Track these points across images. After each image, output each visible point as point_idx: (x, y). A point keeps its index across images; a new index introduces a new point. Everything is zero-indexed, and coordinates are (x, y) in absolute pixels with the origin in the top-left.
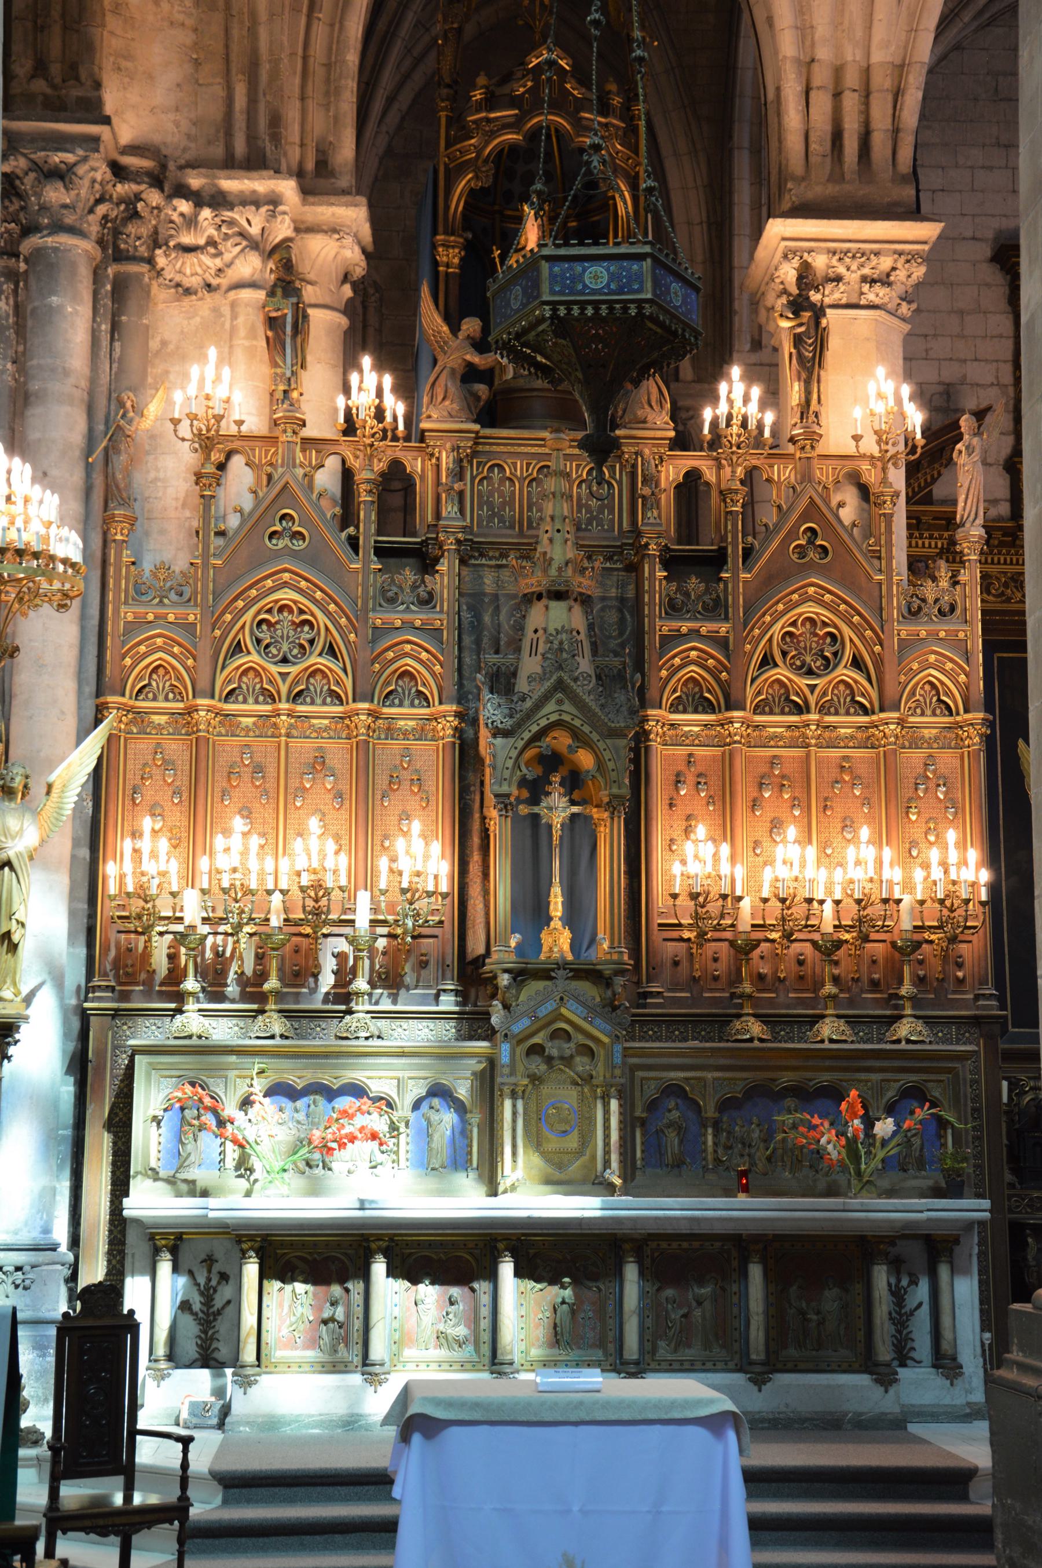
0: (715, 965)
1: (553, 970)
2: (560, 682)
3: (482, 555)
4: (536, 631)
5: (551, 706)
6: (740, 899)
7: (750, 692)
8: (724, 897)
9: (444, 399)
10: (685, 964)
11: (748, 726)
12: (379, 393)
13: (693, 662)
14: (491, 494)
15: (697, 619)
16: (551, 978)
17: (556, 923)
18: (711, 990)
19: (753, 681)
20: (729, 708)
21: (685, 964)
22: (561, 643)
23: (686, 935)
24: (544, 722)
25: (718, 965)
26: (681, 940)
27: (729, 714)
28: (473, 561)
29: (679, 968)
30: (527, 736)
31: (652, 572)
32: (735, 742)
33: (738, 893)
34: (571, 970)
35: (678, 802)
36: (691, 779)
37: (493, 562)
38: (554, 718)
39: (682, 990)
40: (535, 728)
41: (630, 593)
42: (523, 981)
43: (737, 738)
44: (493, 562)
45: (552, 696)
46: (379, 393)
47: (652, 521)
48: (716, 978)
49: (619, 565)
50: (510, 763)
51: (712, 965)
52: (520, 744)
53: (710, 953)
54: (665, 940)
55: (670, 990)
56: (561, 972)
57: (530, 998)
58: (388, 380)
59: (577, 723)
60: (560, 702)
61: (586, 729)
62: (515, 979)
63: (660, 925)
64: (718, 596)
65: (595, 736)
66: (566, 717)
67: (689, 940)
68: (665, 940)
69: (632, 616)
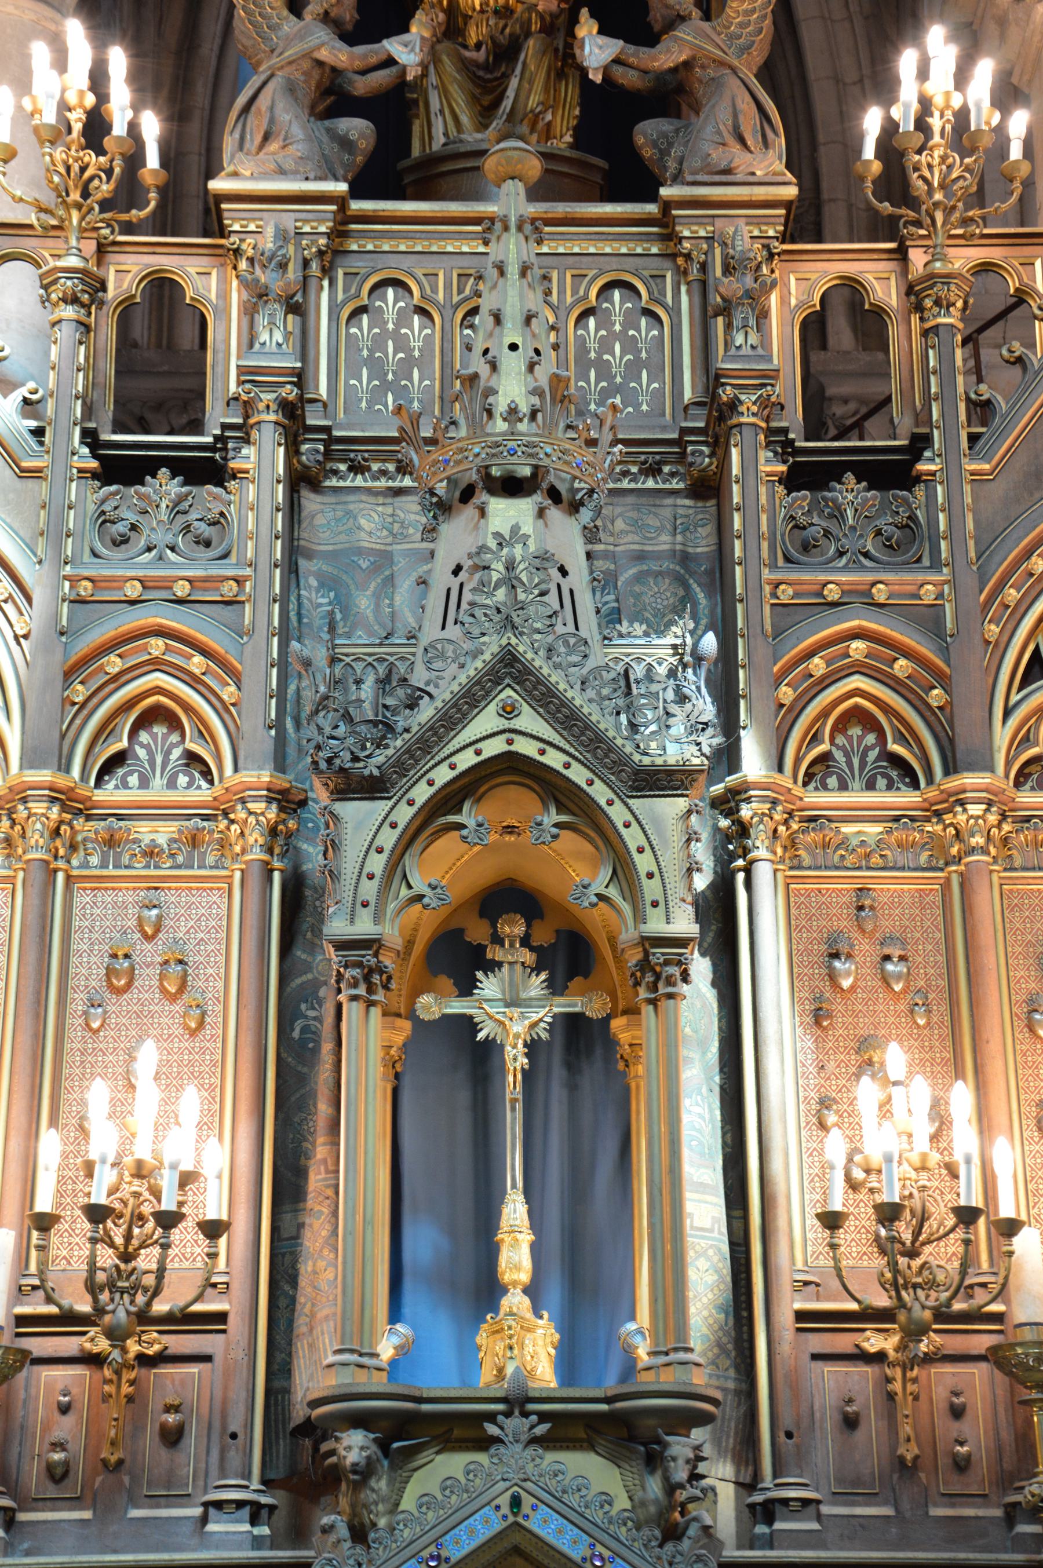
0: (955, 1428)
1: (491, 1417)
2: (509, 659)
3: (356, 469)
4: (457, 571)
5: (487, 720)
6: (1010, 1228)
7: (1002, 736)
8: (967, 1216)
9: (266, 137)
10: (873, 1424)
11: (1004, 817)
12: (98, 80)
13: (858, 669)
14: (379, 343)
15: (863, 568)
16: (485, 1443)
17: (515, 1301)
18: (952, 1498)
19: (1007, 713)
20: (951, 768)
21: (873, 1424)
22: (510, 566)
23: (874, 1342)
24: (467, 760)
25: (964, 1427)
26: (863, 1357)
27: (954, 783)
28: (334, 482)
29: (860, 1434)
30: (422, 793)
31: (749, 464)
32: (972, 851)
33: (1006, 1210)
34: (543, 1417)
35: (838, 1007)
36: (866, 949)
37: (383, 483)
38: (493, 748)
39: (870, 1498)
40: (443, 775)
41: (703, 544)
42: (410, 1453)
43: (978, 840)
44: (383, 483)
45: (487, 696)
46: (98, 80)
47: (746, 351)
48: (962, 1465)
49: (676, 484)
50: (377, 864)
51: (947, 1428)
52: (404, 814)
53: (940, 1394)
54: (815, 1357)
55: (837, 1497)
56: (515, 1424)
57: (426, 1502)
58: (118, 60)
59: (554, 760)
60: (508, 711)
61: (578, 775)
62: (384, 1446)
63: (801, 1316)
64: (913, 518)
65: (600, 793)
66: (526, 748)
67: (880, 1357)
68: (815, 1357)
69: (709, 595)
